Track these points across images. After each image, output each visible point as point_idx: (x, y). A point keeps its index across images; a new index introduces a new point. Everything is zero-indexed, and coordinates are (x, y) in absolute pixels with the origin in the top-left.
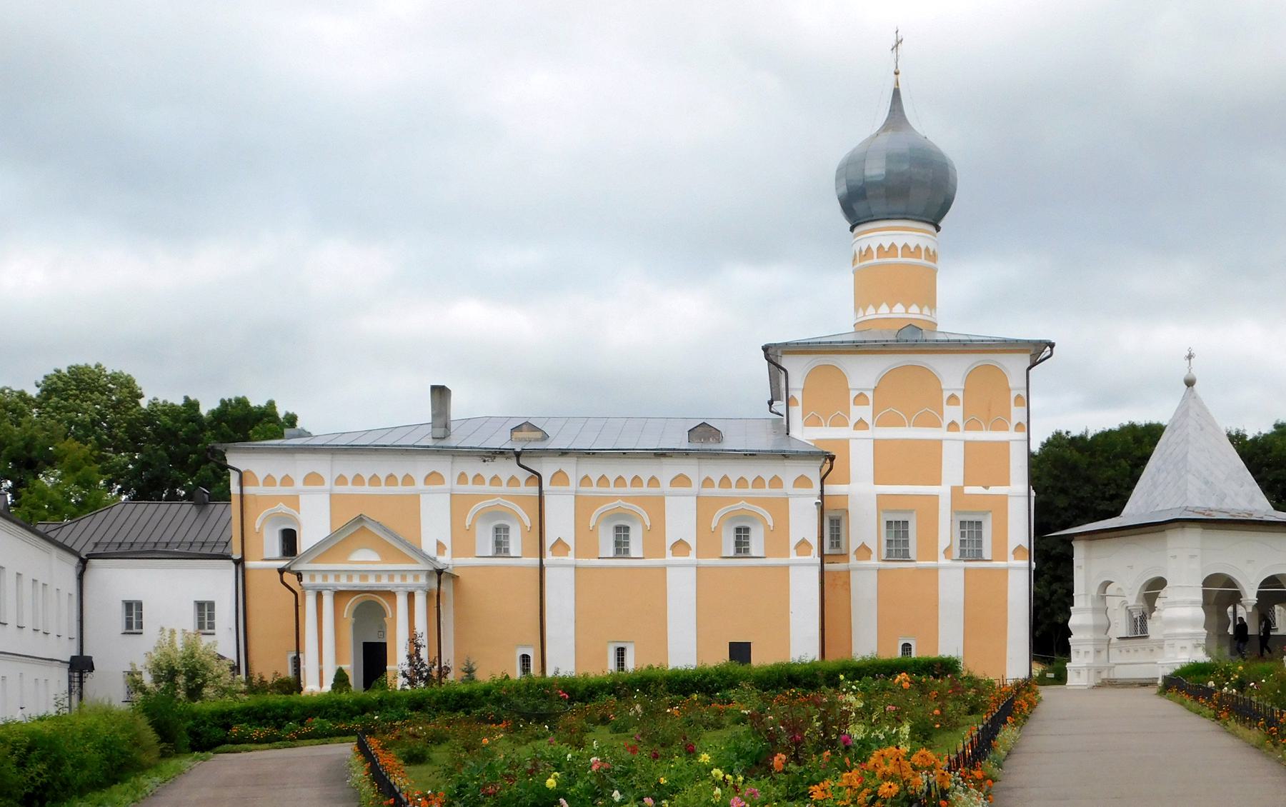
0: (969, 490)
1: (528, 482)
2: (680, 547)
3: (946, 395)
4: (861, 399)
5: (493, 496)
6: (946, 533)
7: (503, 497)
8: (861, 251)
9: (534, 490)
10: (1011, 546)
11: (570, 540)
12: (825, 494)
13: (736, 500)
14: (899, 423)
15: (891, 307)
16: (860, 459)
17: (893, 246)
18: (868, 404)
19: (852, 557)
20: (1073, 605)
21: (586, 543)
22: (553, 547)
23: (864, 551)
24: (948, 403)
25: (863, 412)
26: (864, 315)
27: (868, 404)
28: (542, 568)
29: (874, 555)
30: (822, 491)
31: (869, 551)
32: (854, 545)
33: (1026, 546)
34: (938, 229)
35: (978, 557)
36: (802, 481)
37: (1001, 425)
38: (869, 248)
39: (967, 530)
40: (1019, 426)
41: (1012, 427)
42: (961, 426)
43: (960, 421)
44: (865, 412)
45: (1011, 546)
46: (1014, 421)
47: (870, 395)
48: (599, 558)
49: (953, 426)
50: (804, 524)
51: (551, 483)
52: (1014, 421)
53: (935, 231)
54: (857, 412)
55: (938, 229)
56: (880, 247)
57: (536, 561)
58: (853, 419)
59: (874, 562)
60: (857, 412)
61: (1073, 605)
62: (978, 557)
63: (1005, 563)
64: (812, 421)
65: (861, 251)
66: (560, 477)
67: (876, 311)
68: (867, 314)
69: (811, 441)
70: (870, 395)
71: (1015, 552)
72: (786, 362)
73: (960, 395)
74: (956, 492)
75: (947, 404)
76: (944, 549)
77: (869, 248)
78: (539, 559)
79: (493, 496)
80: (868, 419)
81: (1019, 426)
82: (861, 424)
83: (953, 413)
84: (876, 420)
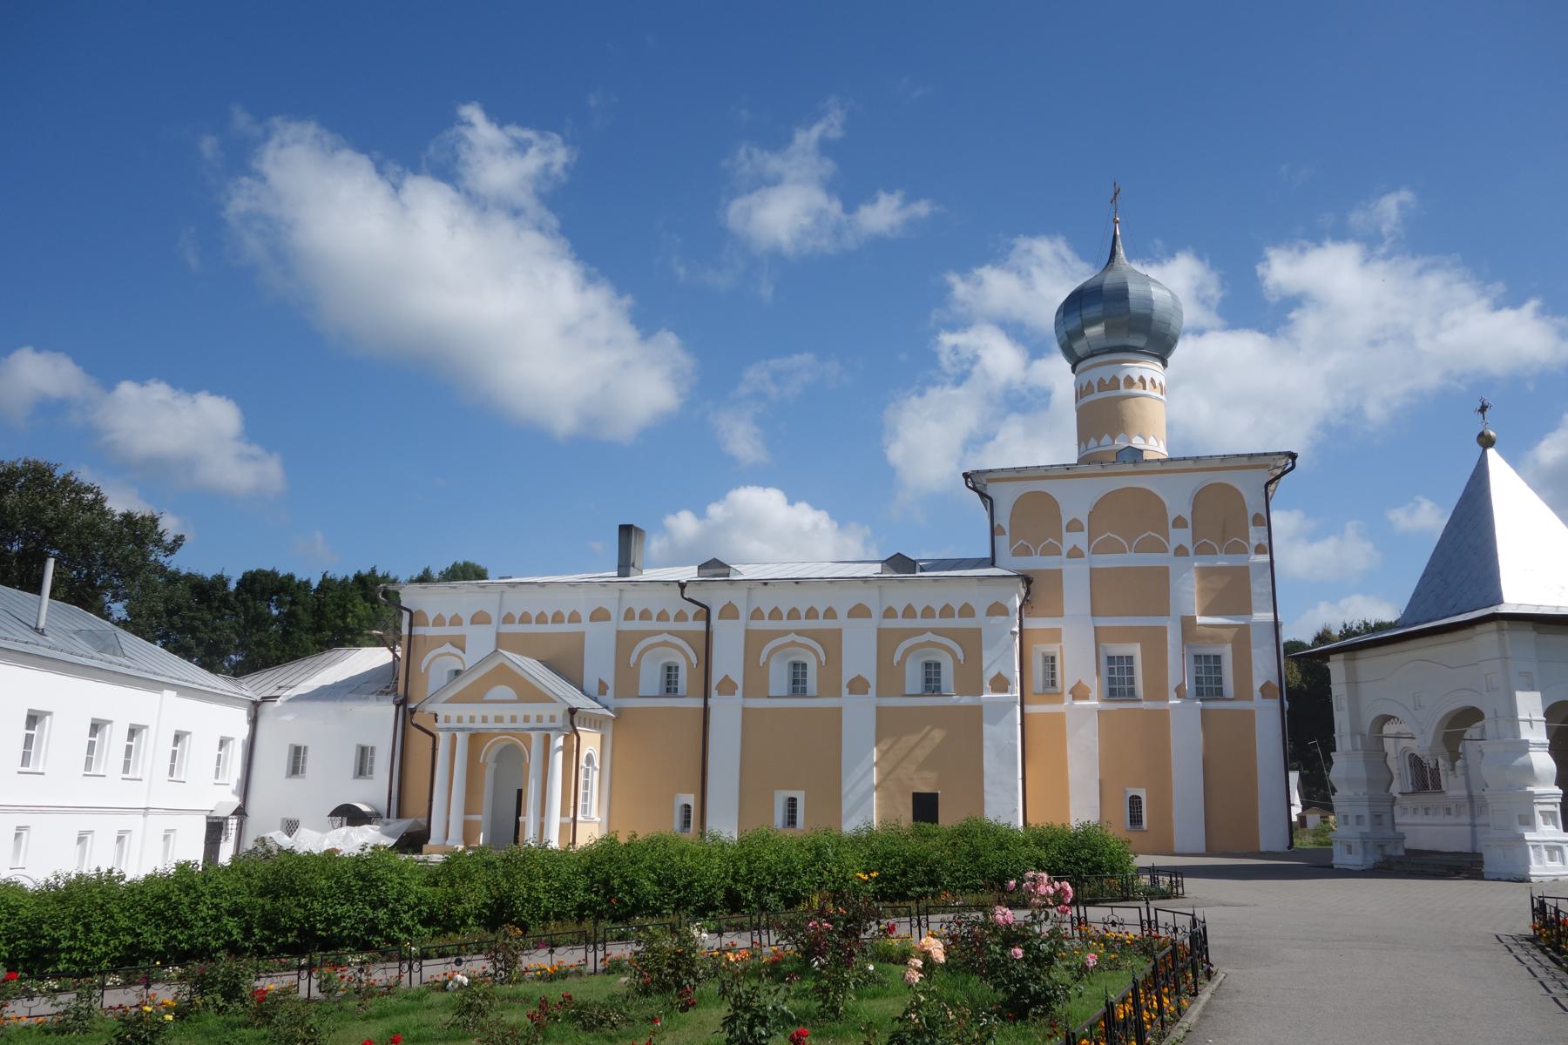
0: (1200, 620)
1: (696, 617)
2: (858, 686)
4: (1075, 526)
5: (660, 632)
6: (1178, 670)
7: (670, 633)
9: (700, 626)
10: (1257, 685)
11: (738, 678)
12: (1024, 627)
18: (1083, 530)
20: (1335, 750)
21: (755, 681)
22: (719, 687)
25: (1080, 540)
28: (706, 710)
33: (1276, 682)
35: (1218, 694)
39: (1203, 666)
42: (1191, 551)
43: (1188, 545)
44: (1080, 540)
45: (1257, 685)
48: (769, 697)
51: (720, 617)
54: (1070, 540)
57: (697, 703)
60: (1070, 540)
61: (1335, 750)
62: (1218, 694)
66: (730, 612)
71: (1262, 690)
75: (1174, 527)
76: (1175, 687)
78: (702, 700)
79: (660, 632)
80: (1084, 547)
82: (1075, 553)
83: (1182, 537)
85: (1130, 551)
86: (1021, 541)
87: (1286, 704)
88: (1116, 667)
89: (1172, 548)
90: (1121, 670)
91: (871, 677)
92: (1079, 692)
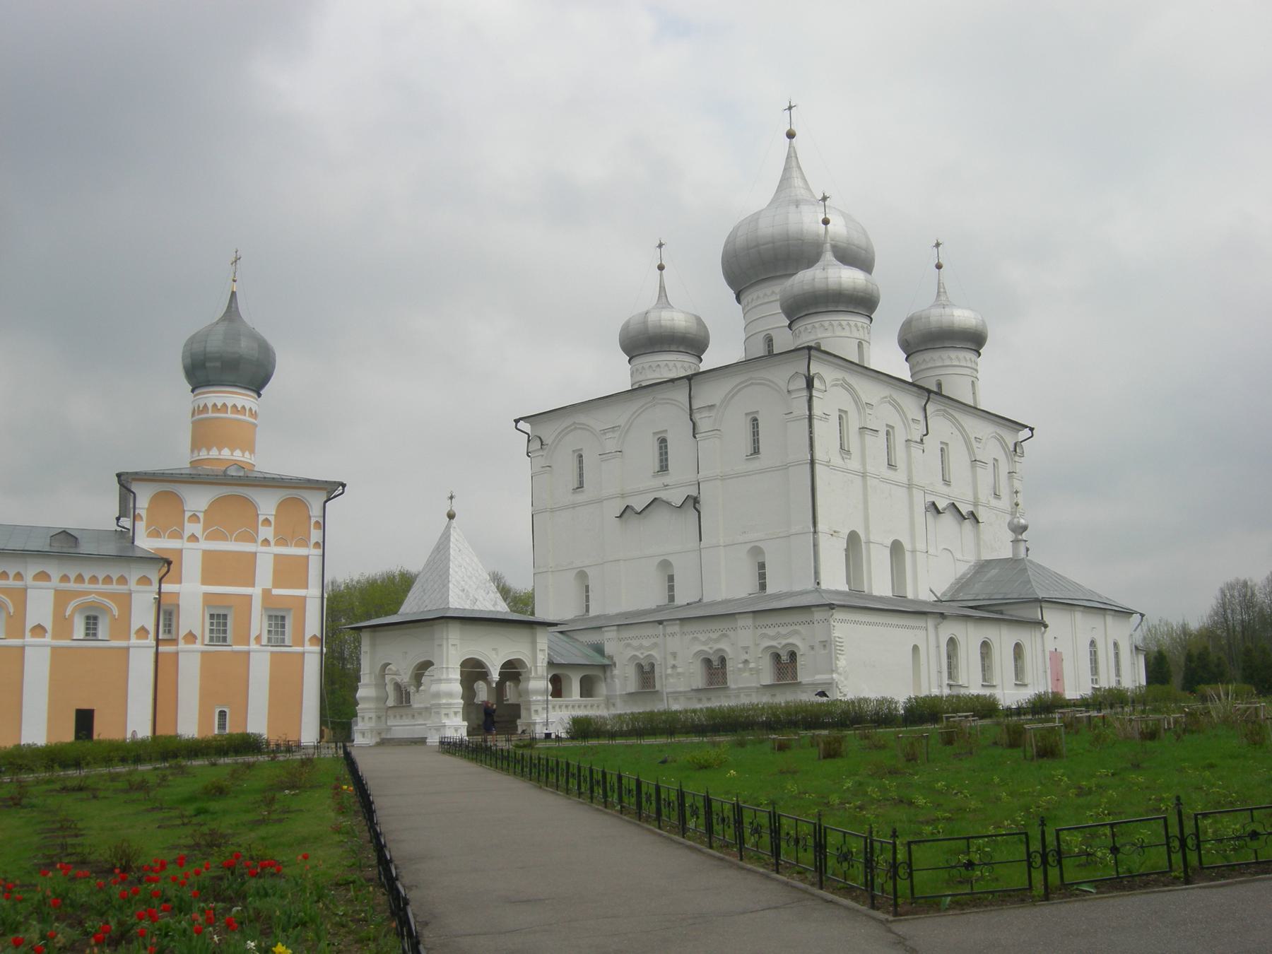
0: (276, 592)
2: (39, 630)
3: (261, 518)
4: (195, 518)
6: (259, 623)
8: (199, 407)
10: (308, 636)
12: (162, 591)
13: (89, 593)
14: (225, 538)
15: (220, 451)
16: (192, 564)
17: (224, 405)
19: (181, 641)
23: (191, 637)
24: (262, 525)
26: (199, 455)
27: (199, 522)
29: (199, 640)
30: (160, 588)
31: (195, 637)
32: (183, 632)
33: (319, 635)
34: (259, 395)
36: (145, 580)
37: (304, 542)
38: (205, 405)
40: (317, 544)
41: (312, 545)
42: (272, 543)
43: (271, 538)
45: (308, 636)
46: (313, 540)
47: (201, 516)
49: (266, 542)
50: (143, 614)
52: (313, 540)
53: (256, 396)
54: (190, 528)
55: (259, 395)
56: (215, 405)
58: (187, 534)
59: (198, 646)
60: (190, 528)
63: (302, 648)
64: (155, 534)
65: (199, 407)
67: (208, 453)
68: (201, 454)
69: (152, 549)
70: (201, 516)
71: (311, 639)
72: (135, 487)
73: (272, 519)
74: (266, 593)
77: (205, 405)
80: (199, 534)
81: (317, 544)
82: (193, 538)
84: (206, 534)
85: (164, 538)
86: (175, 528)
87: (325, 650)
88: (215, 621)
89: (260, 541)
90: (218, 624)
91: (48, 625)
92: (191, 637)
